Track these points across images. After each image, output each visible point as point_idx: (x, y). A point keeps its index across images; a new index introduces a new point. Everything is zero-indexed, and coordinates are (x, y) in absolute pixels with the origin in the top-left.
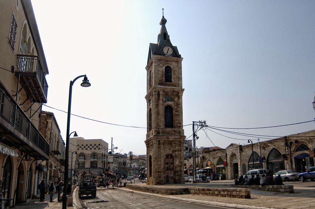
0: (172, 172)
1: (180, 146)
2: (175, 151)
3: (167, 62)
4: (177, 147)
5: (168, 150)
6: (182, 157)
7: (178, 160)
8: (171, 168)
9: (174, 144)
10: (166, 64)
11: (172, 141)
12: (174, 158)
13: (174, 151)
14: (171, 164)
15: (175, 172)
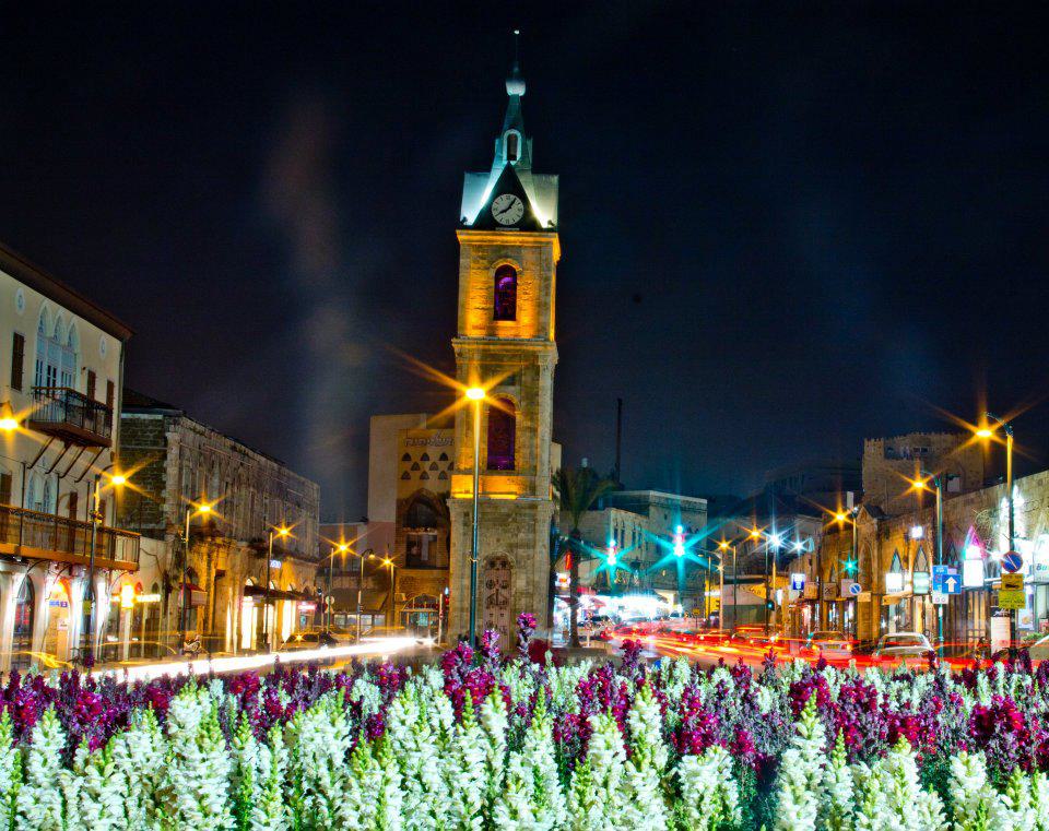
0: (507, 614)
1: (534, 531)
2: (517, 546)
3: (503, 252)
4: (521, 535)
5: (493, 540)
6: (537, 565)
7: (523, 576)
8: (501, 599)
9: (514, 525)
10: (500, 257)
11: (509, 516)
12: (512, 567)
13: (512, 547)
14: (504, 587)
15: (514, 612)
